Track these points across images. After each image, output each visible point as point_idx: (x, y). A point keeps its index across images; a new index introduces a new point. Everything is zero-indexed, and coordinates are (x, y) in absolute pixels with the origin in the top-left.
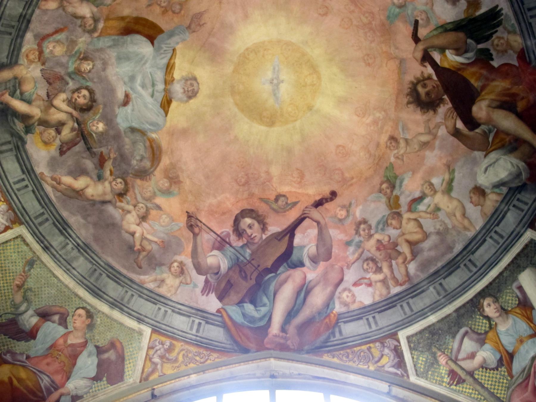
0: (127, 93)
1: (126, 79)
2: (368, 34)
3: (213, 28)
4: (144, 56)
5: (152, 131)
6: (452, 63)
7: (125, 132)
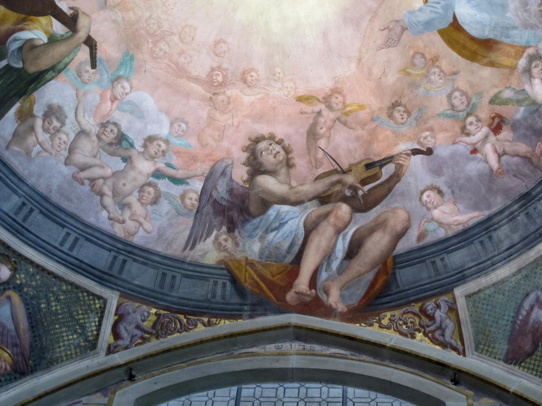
2: (155, 27)
3: (370, 20)
6: (36, 26)
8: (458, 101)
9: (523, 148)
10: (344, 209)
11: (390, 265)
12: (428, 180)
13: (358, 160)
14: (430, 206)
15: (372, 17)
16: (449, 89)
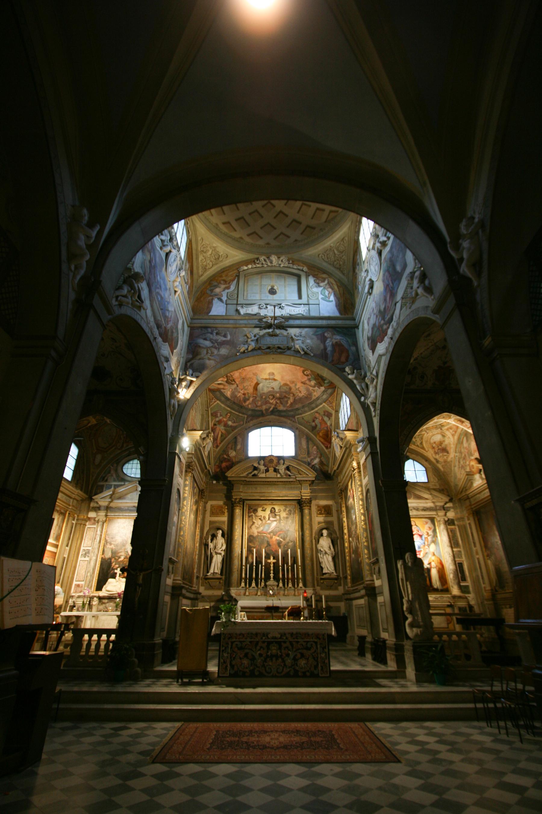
8: (246, 387)
9: (242, 399)
10: (226, 380)
11: (219, 390)
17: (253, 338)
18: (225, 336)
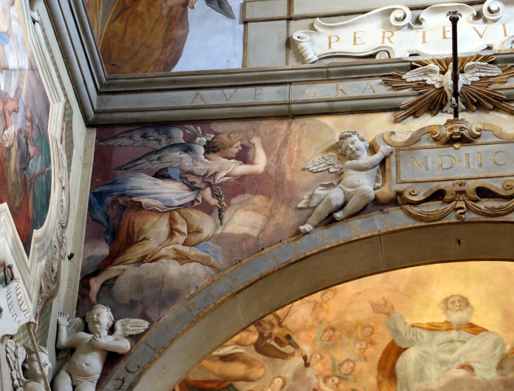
0: (459, 366)
1: (444, 368)
3: (389, 289)
4: (420, 355)
5: (503, 348)
7: (502, 375)
10: (255, 338)
12: (288, 375)
13: (290, 328)
14: (272, 386)
15: (392, 290)
16: (353, 358)
17: (365, 159)
18: (244, 156)
